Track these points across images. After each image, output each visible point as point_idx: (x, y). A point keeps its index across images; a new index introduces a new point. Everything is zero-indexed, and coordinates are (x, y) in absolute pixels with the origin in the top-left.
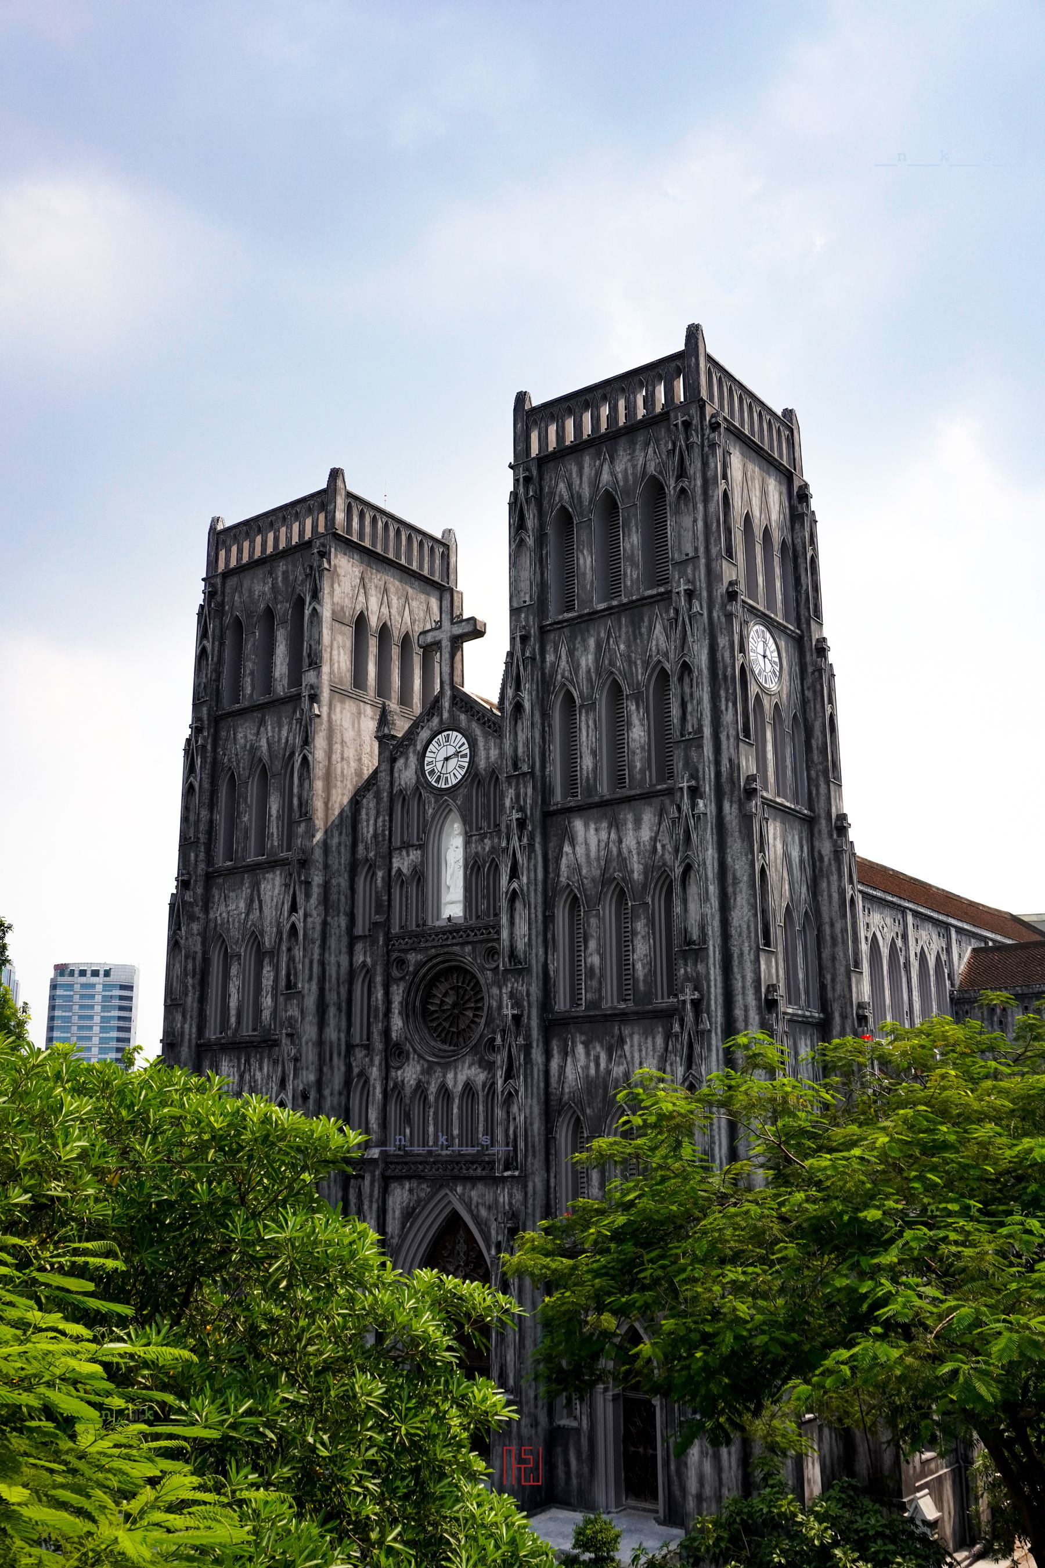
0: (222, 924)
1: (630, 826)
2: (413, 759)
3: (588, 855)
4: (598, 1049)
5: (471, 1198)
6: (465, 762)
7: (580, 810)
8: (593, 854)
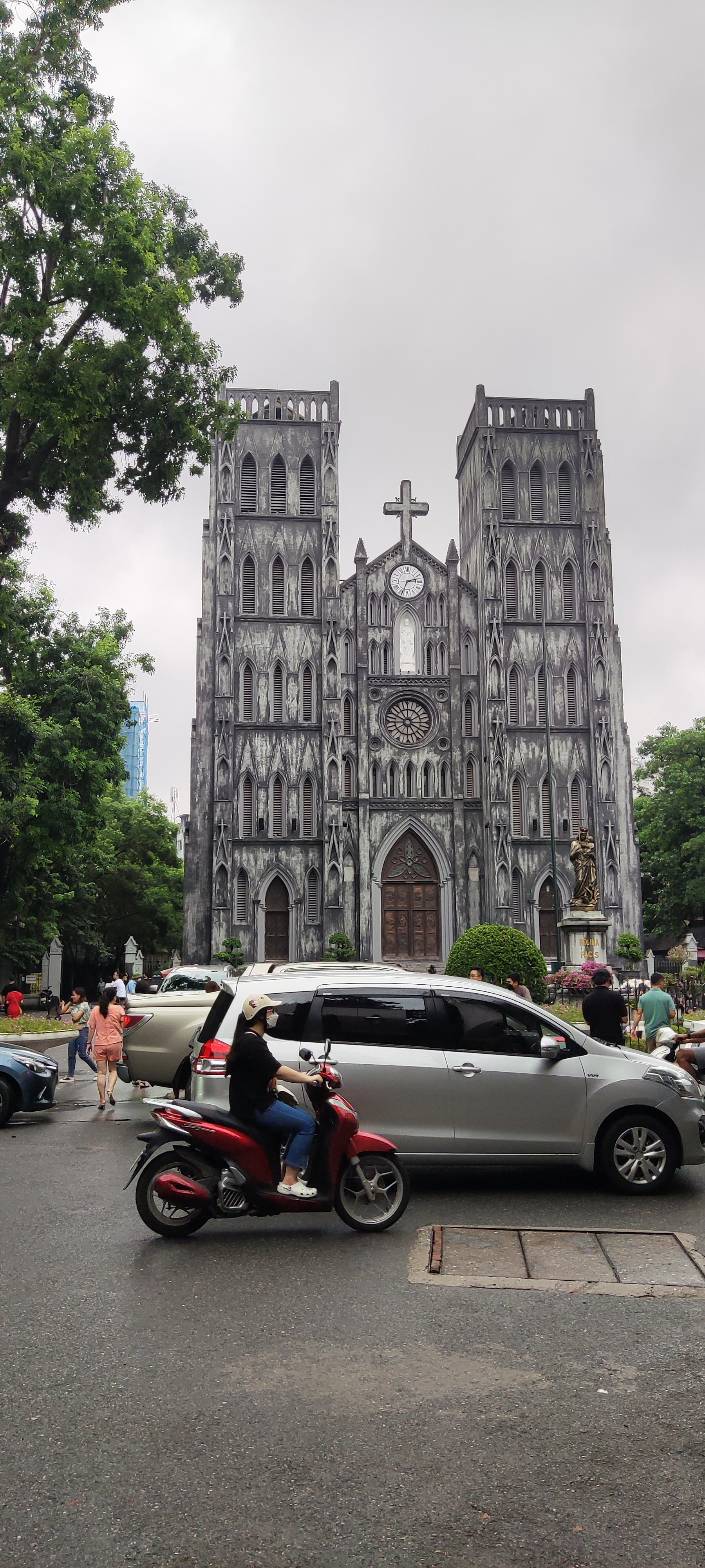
0: (249, 652)
1: (552, 638)
2: (382, 577)
3: (527, 649)
4: (534, 744)
5: (430, 821)
6: (421, 585)
7: (523, 625)
8: (530, 649)
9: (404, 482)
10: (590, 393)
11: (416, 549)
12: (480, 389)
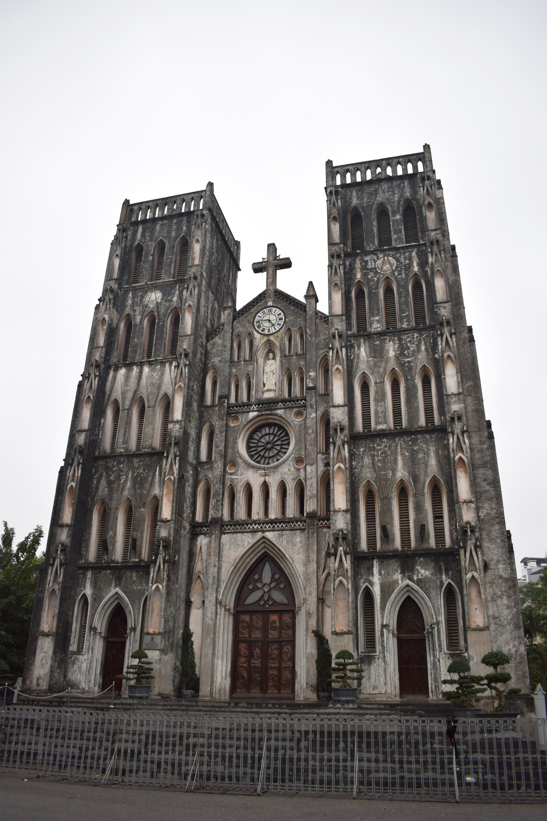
9: (269, 245)
10: (427, 147)
12: (329, 163)
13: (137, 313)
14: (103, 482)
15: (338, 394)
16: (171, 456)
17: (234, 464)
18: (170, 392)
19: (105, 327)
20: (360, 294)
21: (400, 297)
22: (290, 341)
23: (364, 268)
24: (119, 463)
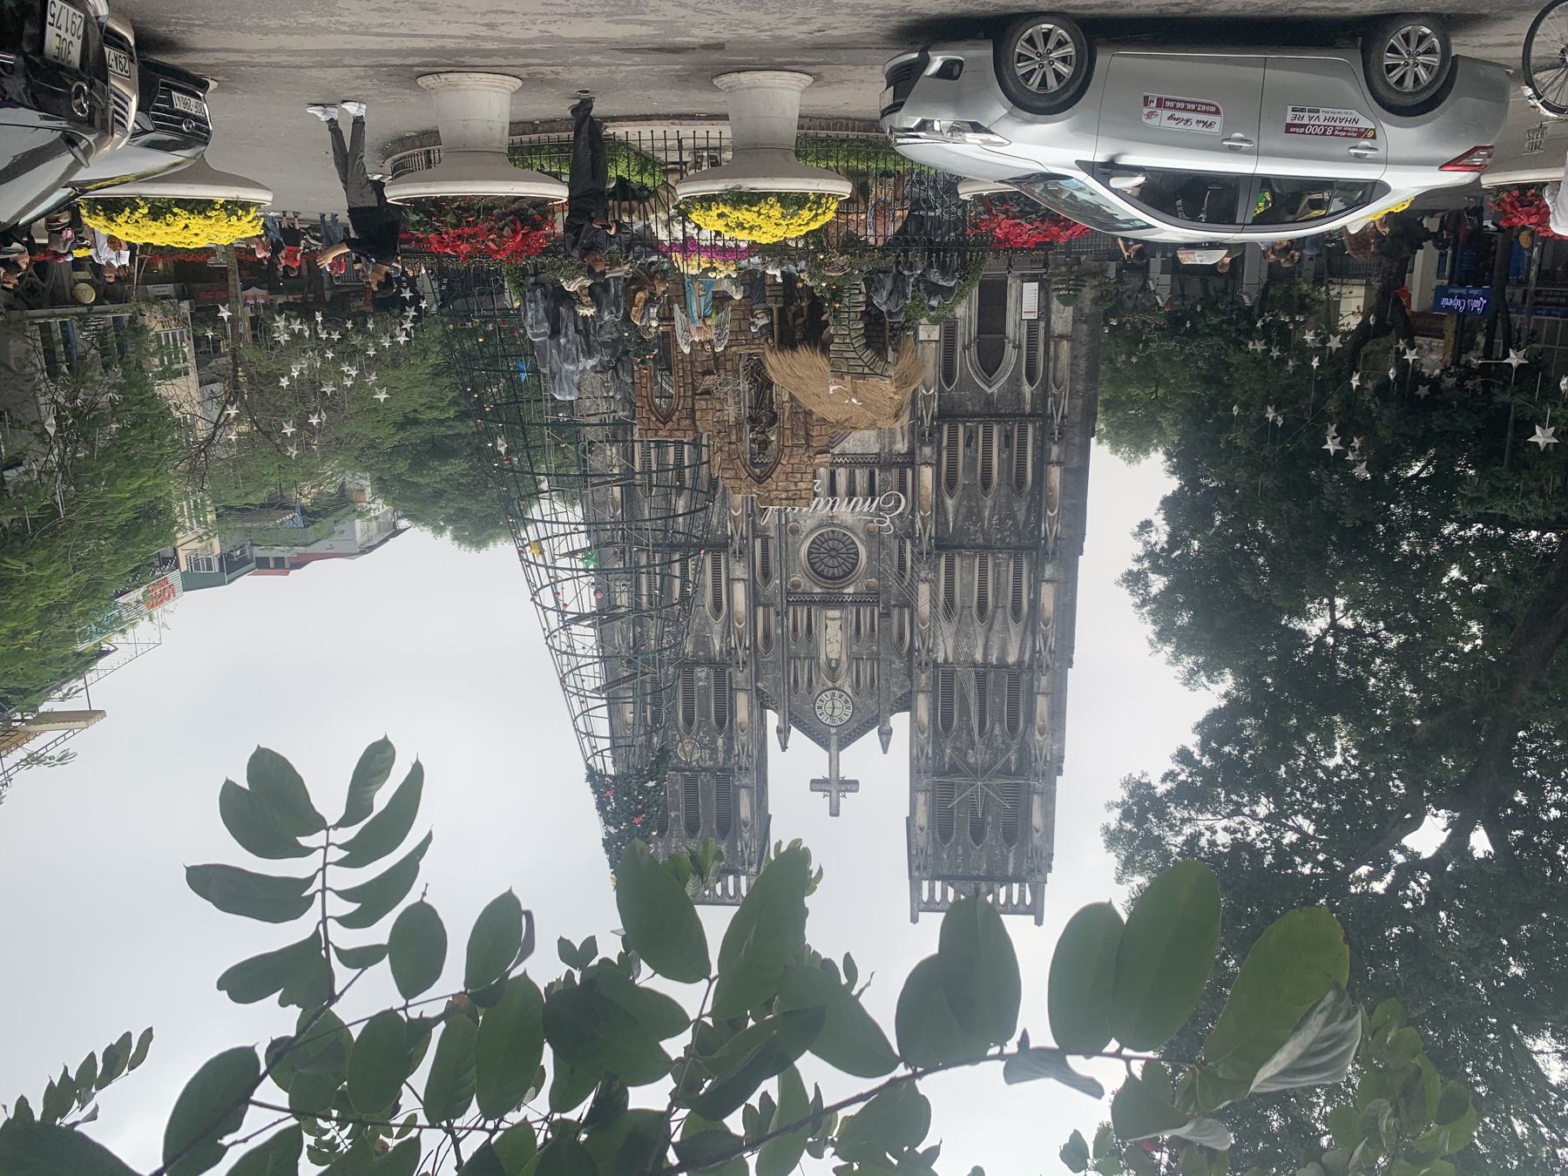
11: (824, 744)
13: (1000, 739)
14: (1021, 516)
15: (740, 591)
16: (925, 539)
17: (869, 533)
18: (944, 624)
19: (1039, 722)
20: (720, 722)
21: (674, 707)
22: (810, 681)
23: (714, 751)
24: (1002, 540)
